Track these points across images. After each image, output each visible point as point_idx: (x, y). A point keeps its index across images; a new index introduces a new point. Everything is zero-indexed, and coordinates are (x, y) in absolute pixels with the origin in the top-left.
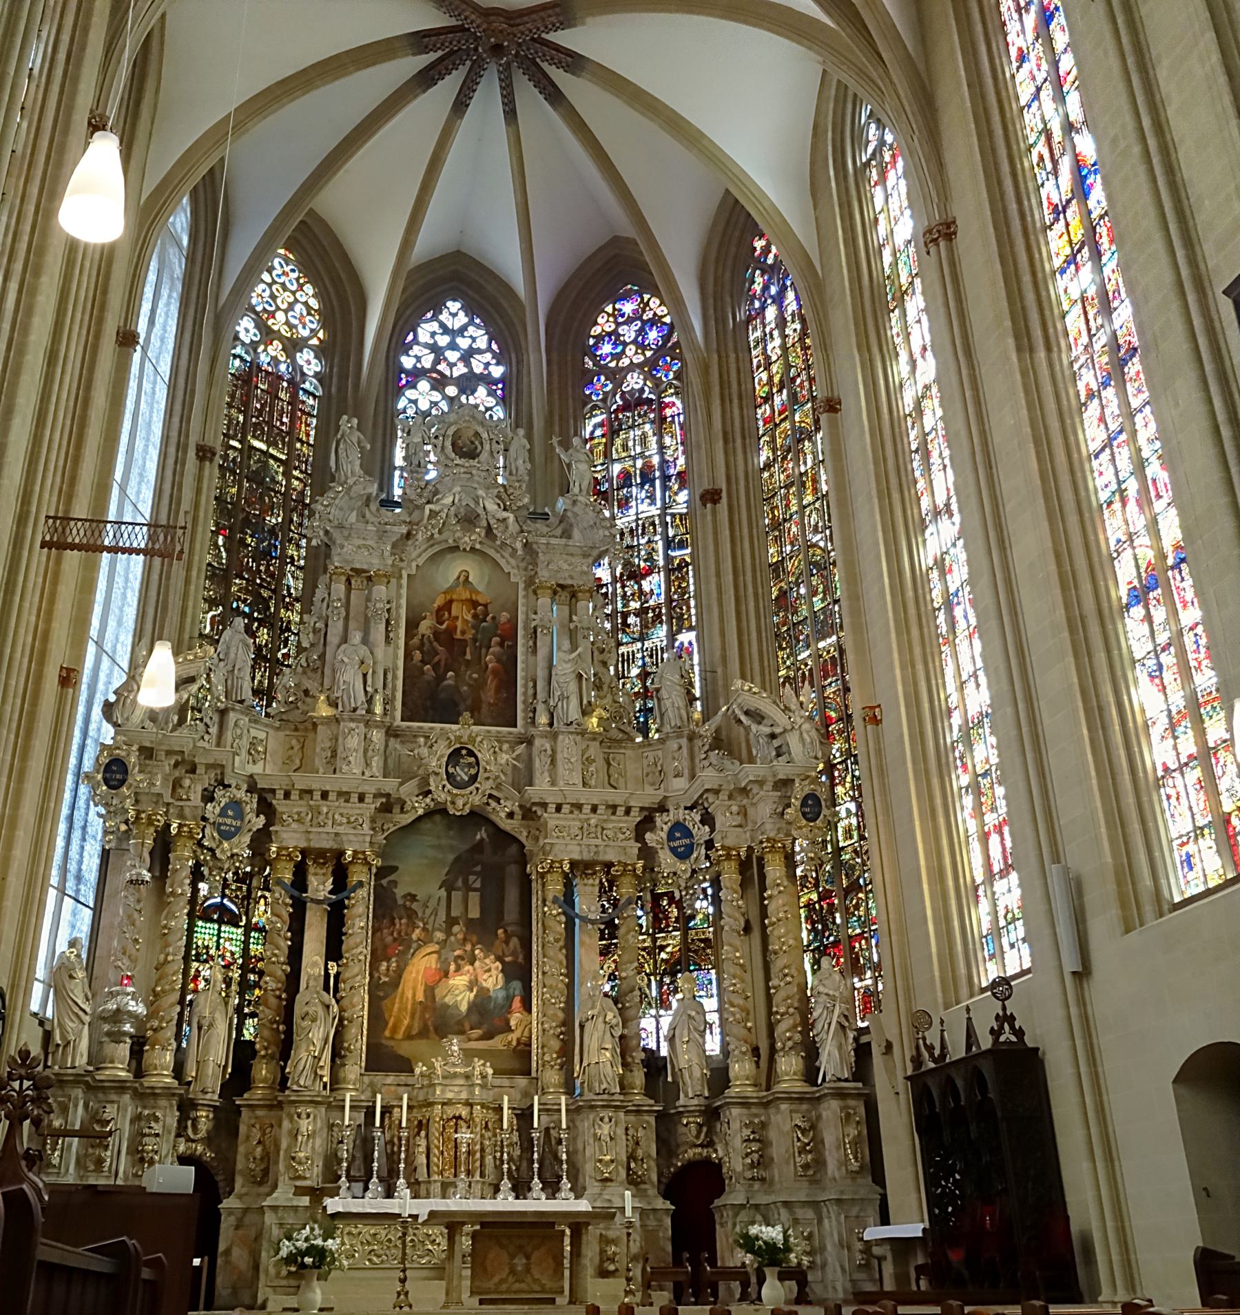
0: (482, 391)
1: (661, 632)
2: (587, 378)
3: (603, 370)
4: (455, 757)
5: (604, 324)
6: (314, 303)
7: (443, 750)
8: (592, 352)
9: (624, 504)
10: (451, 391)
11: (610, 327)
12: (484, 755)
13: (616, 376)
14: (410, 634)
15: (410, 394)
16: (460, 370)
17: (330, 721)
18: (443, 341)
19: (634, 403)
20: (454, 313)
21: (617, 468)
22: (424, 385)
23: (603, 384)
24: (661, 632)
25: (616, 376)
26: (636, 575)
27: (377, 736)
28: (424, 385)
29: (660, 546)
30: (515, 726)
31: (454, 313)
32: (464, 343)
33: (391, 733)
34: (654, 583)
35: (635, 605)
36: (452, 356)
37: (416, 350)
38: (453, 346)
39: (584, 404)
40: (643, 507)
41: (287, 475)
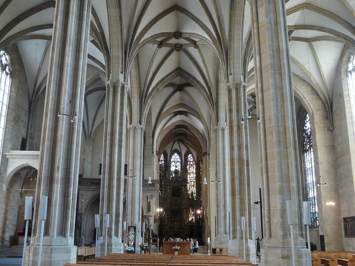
0: (178, 163)
1: (193, 187)
2: (188, 162)
3: (189, 161)
4: (175, 200)
5: (189, 156)
6: (163, 156)
7: (175, 200)
8: (188, 159)
9: (190, 175)
10: (176, 163)
11: (190, 157)
12: (177, 200)
13: (190, 162)
14: (172, 190)
15: (172, 163)
16: (177, 160)
17: (166, 198)
18: (175, 158)
19: (191, 165)
20: (176, 154)
21: (190, 171)
22: (173, 162)
23: (189, 163)
24: (193, 187)
25: (190, 162)
26: (191, 182)
27: (170, 199)
28: (173, 162)
29: (193, 179)
30: (180, 197)
31: (176, 154)
32: (177, 158)
33: (170, 198)
34: (192, 183)
35: (191, 185)
36: (176, 159)
37: (172, 159)
38: (176, 158)
39: (187, 165)
40: (192, 175)
41: (162, 174)
